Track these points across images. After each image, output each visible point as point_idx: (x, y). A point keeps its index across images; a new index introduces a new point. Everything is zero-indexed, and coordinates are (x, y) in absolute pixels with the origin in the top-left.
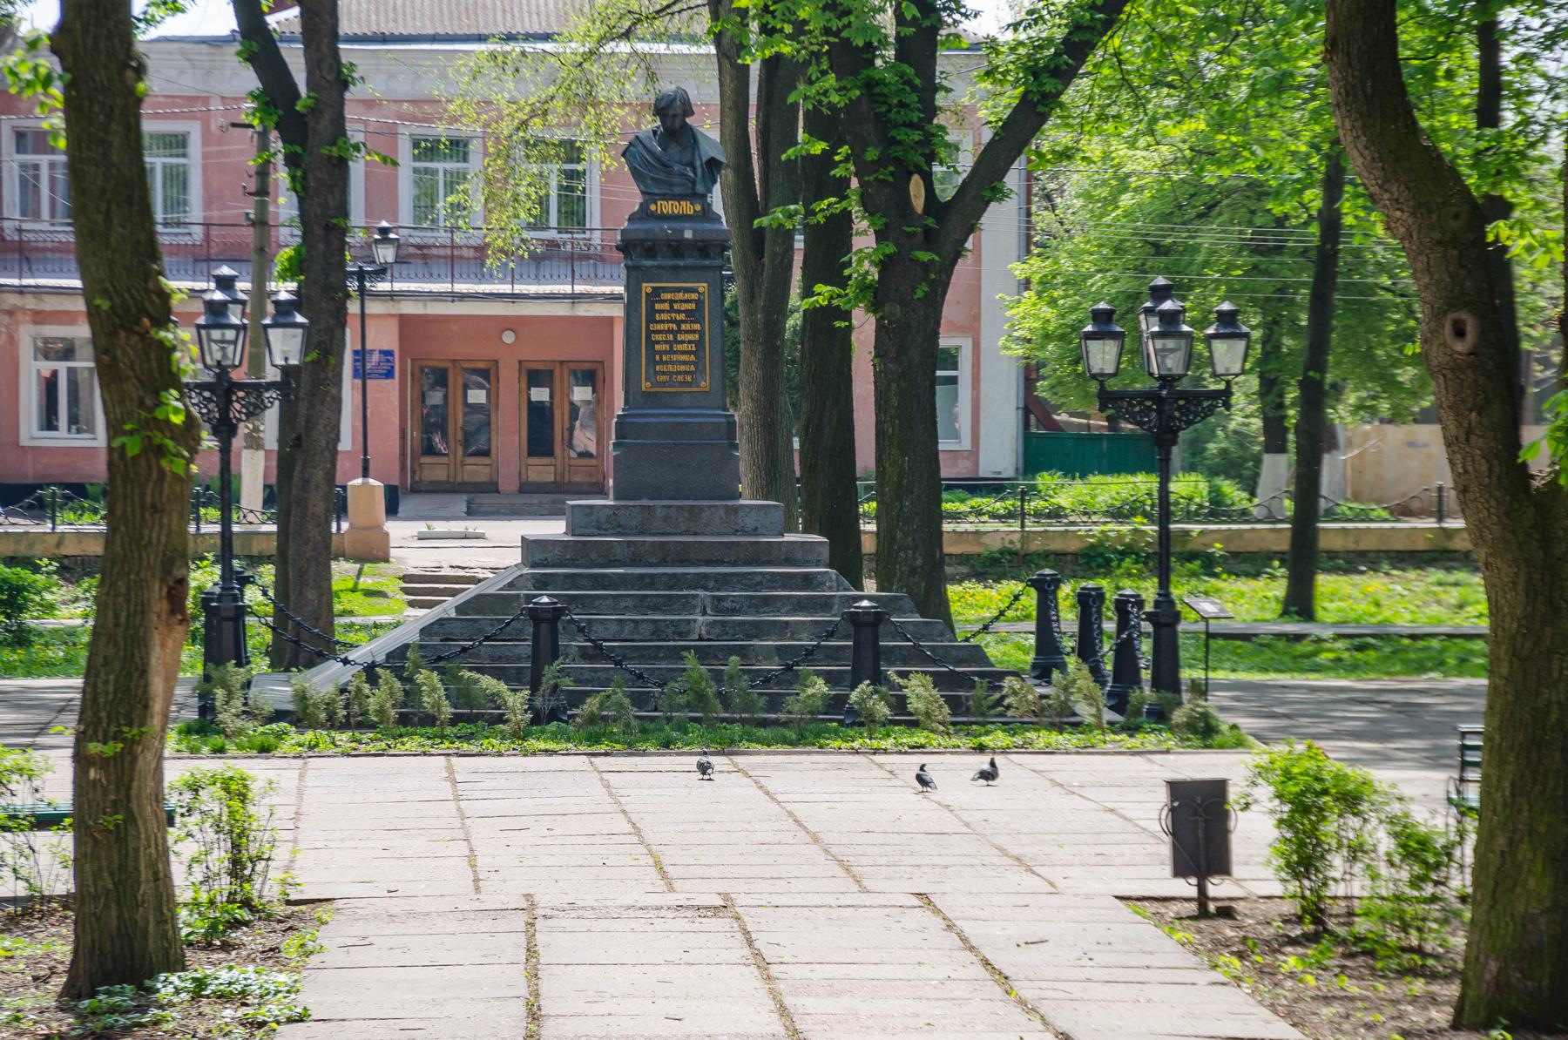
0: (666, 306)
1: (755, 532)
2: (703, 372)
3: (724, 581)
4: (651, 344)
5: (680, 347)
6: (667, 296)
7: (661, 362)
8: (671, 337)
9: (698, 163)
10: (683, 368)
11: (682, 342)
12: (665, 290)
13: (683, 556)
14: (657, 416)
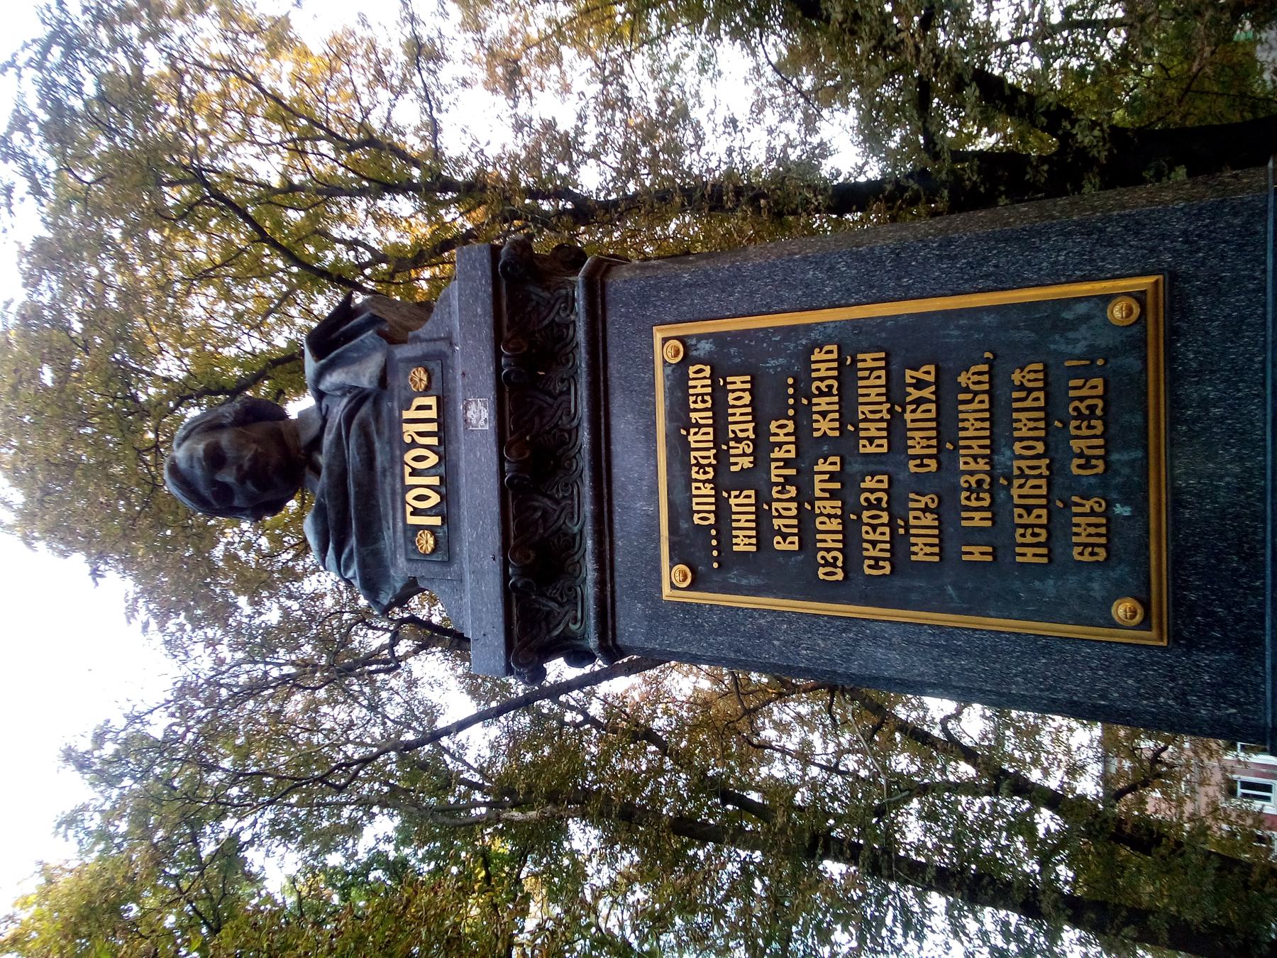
0: (741, 502)
2: (1050, 319)
5: (918, 443)
7: (999, 535)
10: (1026, 424)
11: (895, 428)
12: (681, 510)
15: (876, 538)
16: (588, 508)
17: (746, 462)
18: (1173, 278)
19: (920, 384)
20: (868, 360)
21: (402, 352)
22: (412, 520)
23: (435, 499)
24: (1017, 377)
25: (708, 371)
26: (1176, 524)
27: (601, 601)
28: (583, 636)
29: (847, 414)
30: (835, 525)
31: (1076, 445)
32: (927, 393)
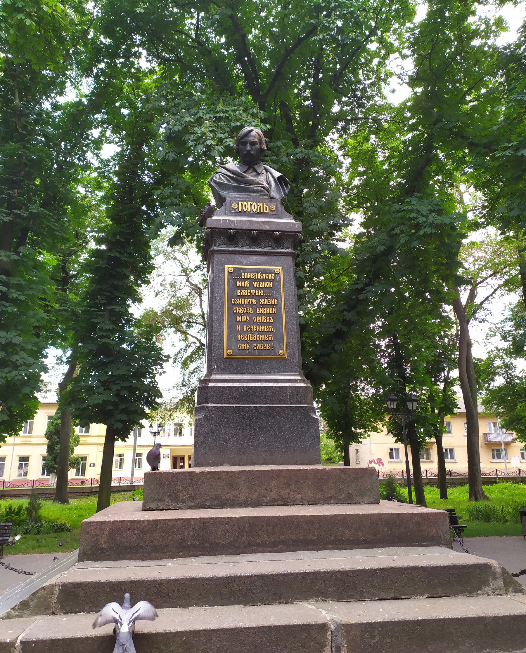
0: (247, 284)
2: (281, 341)
4: (233, 315)
5: (259, 319)
6: (248, 276)
8: (251, 310)
10: (262, 337)
11: (262, 314)
15: (241, 310)
17: (255, 285)
18: (286, 360)
19: (270, 319)
20: (274, 310)
21: (279, 205)
22: (240, 203)
23: (245, 210)
24: (271, 336)
25: (273, 278)
26: (245, 360)
27: (225, 251)
28: (215, 246)
29: (264, 306)
30: (243, 302)
31: (259, 345)
32: (268, 320)
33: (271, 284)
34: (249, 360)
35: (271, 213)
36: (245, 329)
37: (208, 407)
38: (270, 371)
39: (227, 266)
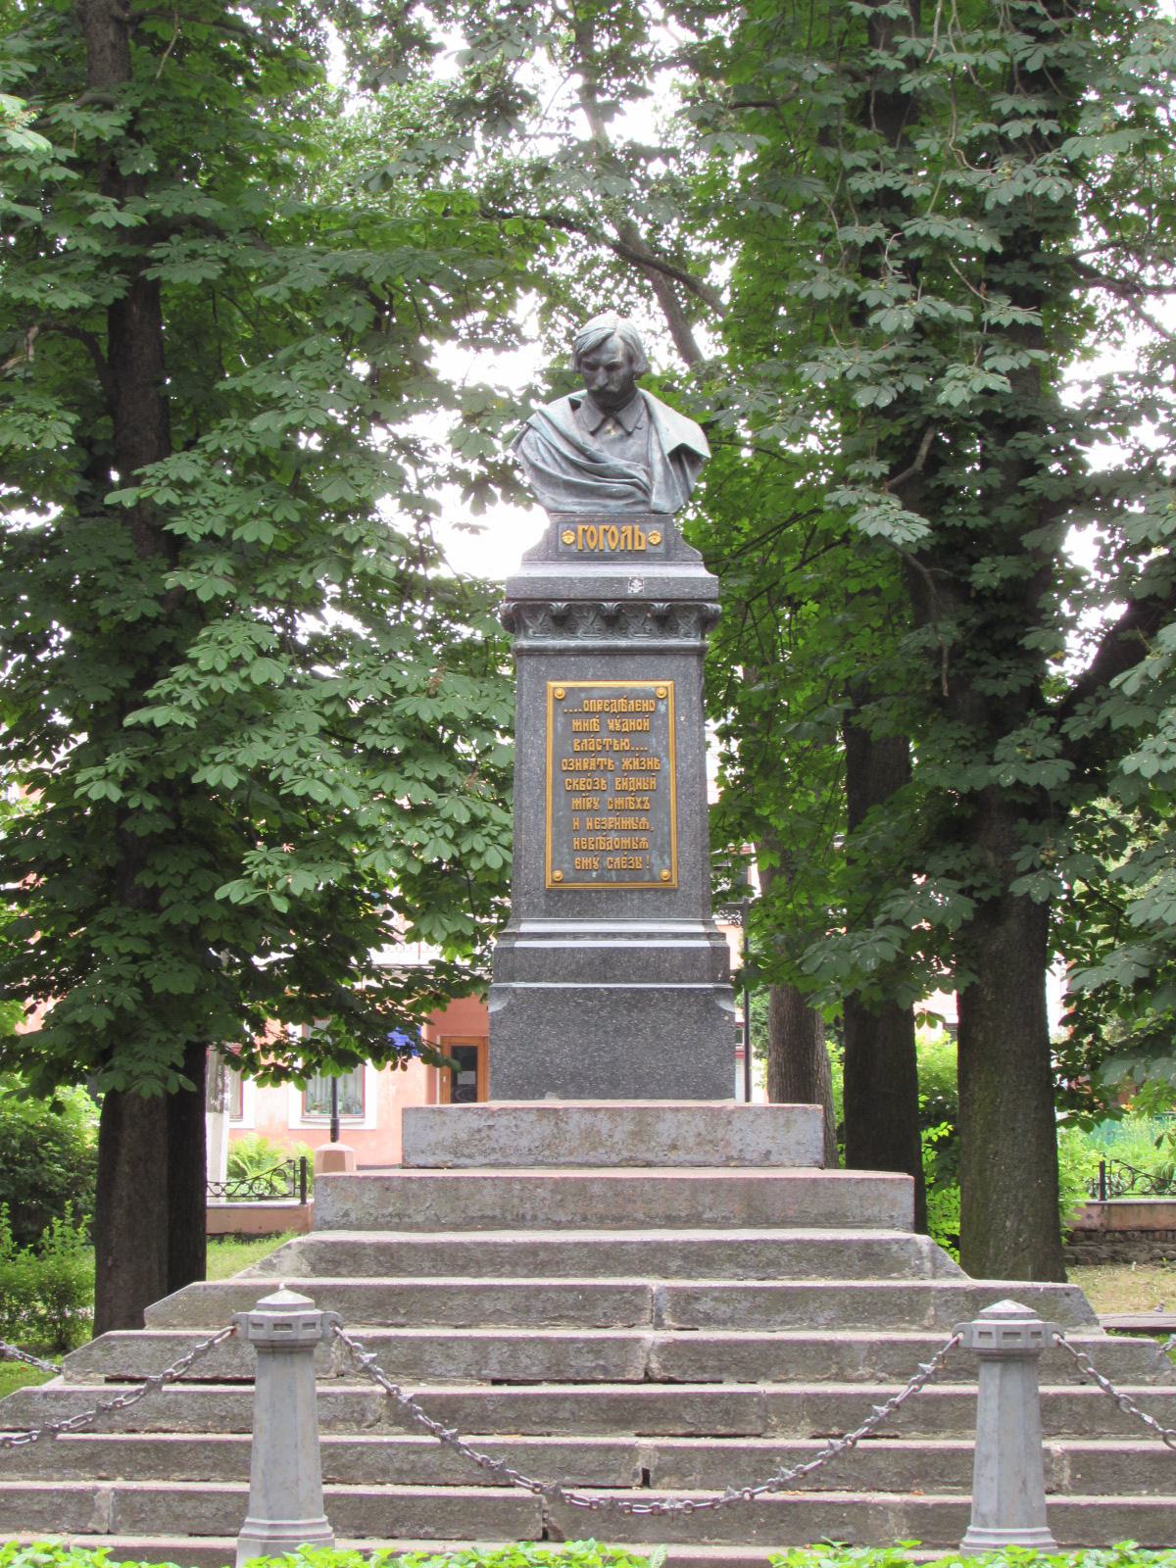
0: (593, 724)
1: (765, 1160)
2: (664, 850)
3: (699, 1258)
5: (619, 801)
9: (656, 456)
10: (626, 841)
13: (620, 1206)
14: (575, 936)
15: (580, 783)
16: (590, 643)
26: (590, 892)
28: (527, 637)
33: (647, 724)
34: (597, 892)
35: (652, 549)
36: (589, 825)
37: (514, 990)
38: (641, 915)
39: (553, 684)
